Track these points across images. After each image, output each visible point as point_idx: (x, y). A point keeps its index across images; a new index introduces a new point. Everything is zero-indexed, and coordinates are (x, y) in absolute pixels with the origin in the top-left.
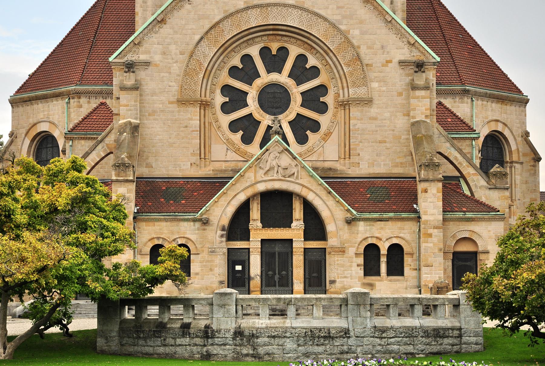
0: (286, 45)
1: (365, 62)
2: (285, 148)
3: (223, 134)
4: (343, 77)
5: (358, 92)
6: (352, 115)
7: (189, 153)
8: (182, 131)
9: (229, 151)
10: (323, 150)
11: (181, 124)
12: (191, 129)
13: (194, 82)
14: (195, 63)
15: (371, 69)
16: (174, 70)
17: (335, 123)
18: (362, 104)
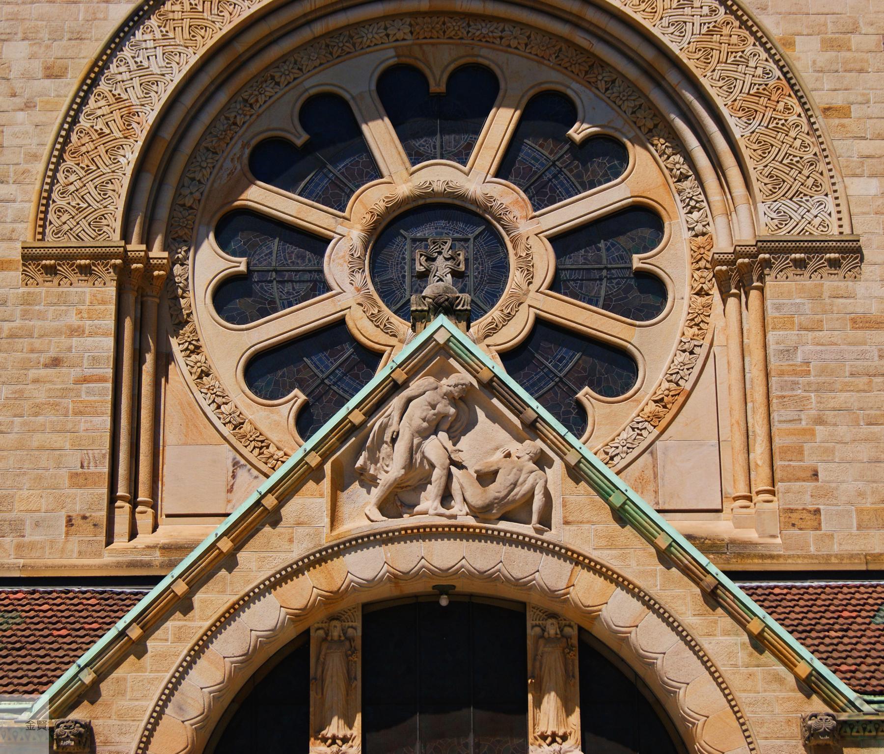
0: (488, 56)
1: (819, 99)
2: (485, 376)
3: (219, 400)
4: (728, 160)
5: (796, 217)
6: (778, 308)
7: (64, 472)
8: (36, 381)
9: (242, 474)
10: (655, 466)
11: (32, 351)
12: (75, 373)
13: (97, 181)
14: (106, 110)
15: (843, 126)
16: (15, 135)
17: (701, 352)
18: (812, 265)
